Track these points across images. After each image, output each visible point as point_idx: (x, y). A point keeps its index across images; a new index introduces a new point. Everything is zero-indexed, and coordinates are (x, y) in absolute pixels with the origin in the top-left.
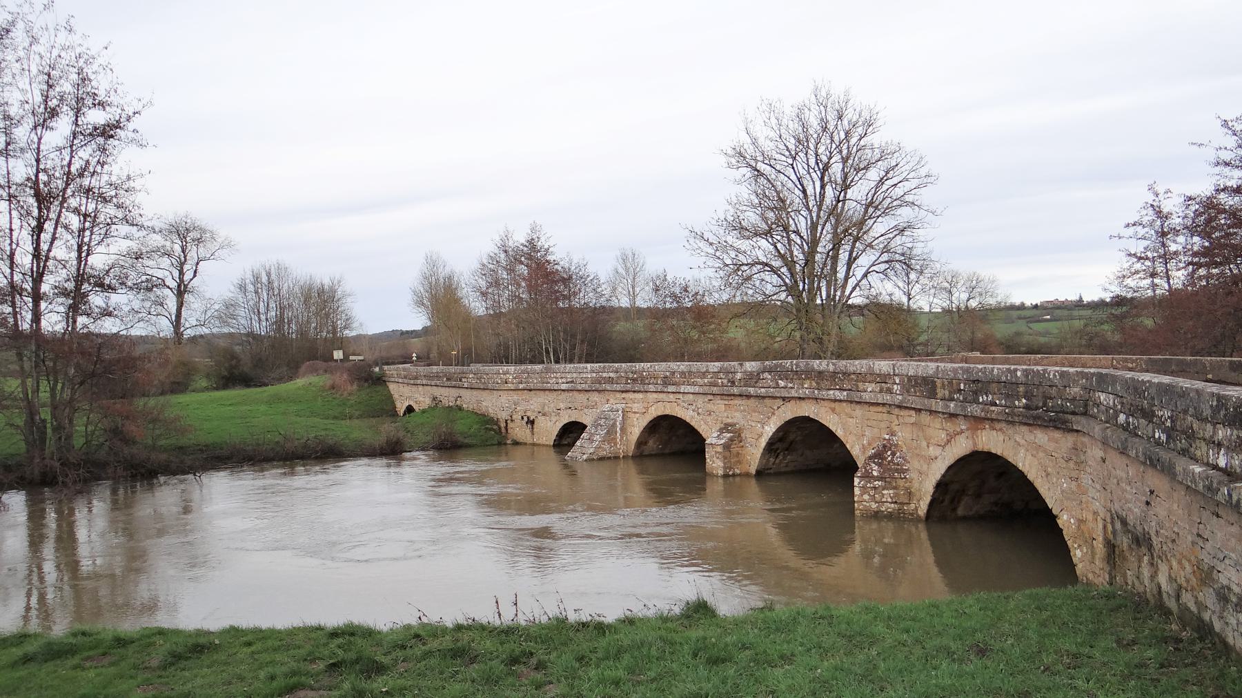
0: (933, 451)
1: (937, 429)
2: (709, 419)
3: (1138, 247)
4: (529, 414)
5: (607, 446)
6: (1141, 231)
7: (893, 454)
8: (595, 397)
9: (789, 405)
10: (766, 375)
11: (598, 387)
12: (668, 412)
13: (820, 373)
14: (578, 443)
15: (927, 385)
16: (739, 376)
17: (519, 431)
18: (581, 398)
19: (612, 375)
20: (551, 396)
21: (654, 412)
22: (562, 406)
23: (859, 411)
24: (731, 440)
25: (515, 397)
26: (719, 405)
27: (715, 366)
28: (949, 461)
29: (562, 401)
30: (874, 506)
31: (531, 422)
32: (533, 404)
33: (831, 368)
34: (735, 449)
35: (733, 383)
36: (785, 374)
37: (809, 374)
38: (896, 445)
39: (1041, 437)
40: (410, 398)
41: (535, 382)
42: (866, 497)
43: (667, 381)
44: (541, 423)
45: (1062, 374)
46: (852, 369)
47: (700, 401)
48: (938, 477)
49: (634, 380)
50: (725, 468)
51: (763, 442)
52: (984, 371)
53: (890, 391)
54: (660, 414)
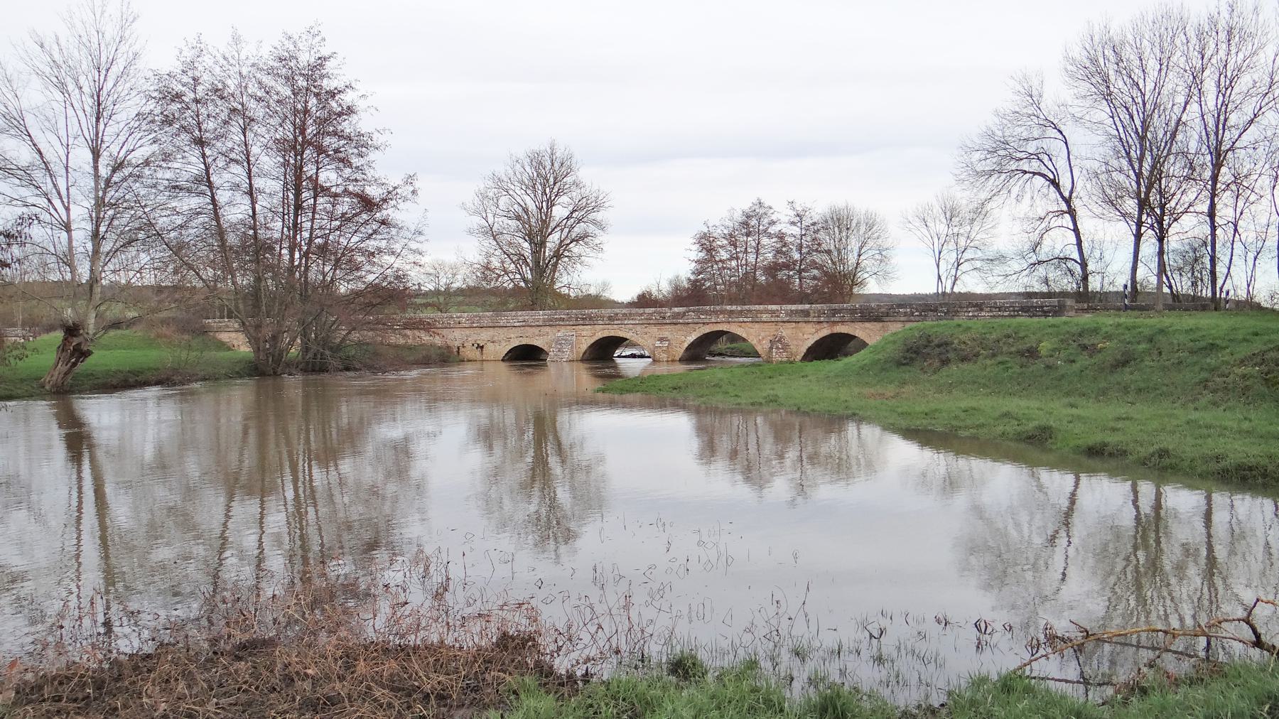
1: (810, 328)
8: (547, 329)
11: (550, 323)
15: (806, 313)
17: (470, 352)
18: (536, 330)
20: (500, 330)
21: (599, 335)
23: (757, 326)
25: (468, 332)
26: (654, 330)
27: (651, 310)
29: (513, 334)
32: (483, 336)
36: (706, 313)
37: (722, 312)
39: (867, 325)
41: (485, 322)
43: (610, 318)
44: (490, 348)
47: (638, 328)
51: (686, 345)
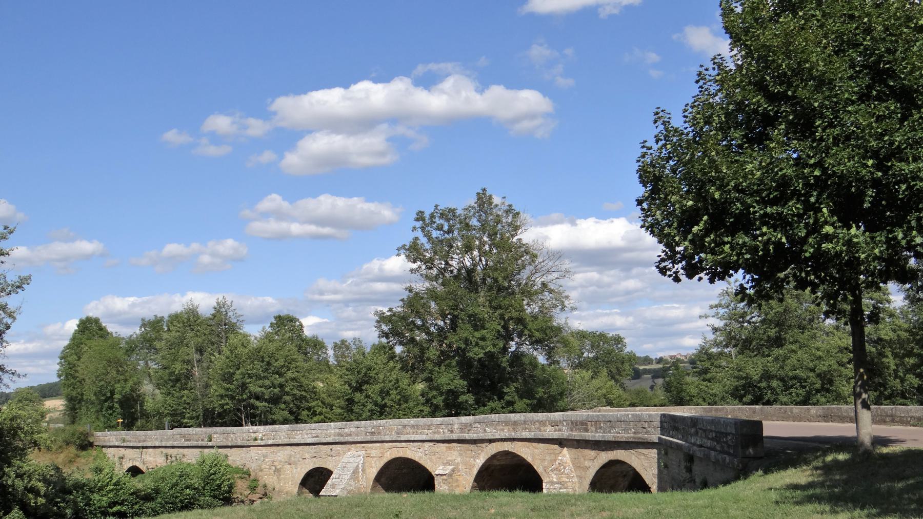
0: (587, 463)
2: (434, 457)
3: (719, 324)
4: (276, 463)
5: (352, 483)
6: (721, 311)
7: (565, 468)
9: (494, 444)
12: (401, 455)
14: (329, 482)
16: (456, 426)
19: (353, 430)
22: (307, 456)
24: (453, 470)
28: (597, 468)
29: (308, 451)
31: (277, 471)
33: (523, 418)
34: (455, 477)
40: (134, 459)
45: (650, 415)
46: (536, 419)
48: (591, 477)
49: (372, 433)
52: (613, 416)
53: (560, 430)
54: (394, 457)
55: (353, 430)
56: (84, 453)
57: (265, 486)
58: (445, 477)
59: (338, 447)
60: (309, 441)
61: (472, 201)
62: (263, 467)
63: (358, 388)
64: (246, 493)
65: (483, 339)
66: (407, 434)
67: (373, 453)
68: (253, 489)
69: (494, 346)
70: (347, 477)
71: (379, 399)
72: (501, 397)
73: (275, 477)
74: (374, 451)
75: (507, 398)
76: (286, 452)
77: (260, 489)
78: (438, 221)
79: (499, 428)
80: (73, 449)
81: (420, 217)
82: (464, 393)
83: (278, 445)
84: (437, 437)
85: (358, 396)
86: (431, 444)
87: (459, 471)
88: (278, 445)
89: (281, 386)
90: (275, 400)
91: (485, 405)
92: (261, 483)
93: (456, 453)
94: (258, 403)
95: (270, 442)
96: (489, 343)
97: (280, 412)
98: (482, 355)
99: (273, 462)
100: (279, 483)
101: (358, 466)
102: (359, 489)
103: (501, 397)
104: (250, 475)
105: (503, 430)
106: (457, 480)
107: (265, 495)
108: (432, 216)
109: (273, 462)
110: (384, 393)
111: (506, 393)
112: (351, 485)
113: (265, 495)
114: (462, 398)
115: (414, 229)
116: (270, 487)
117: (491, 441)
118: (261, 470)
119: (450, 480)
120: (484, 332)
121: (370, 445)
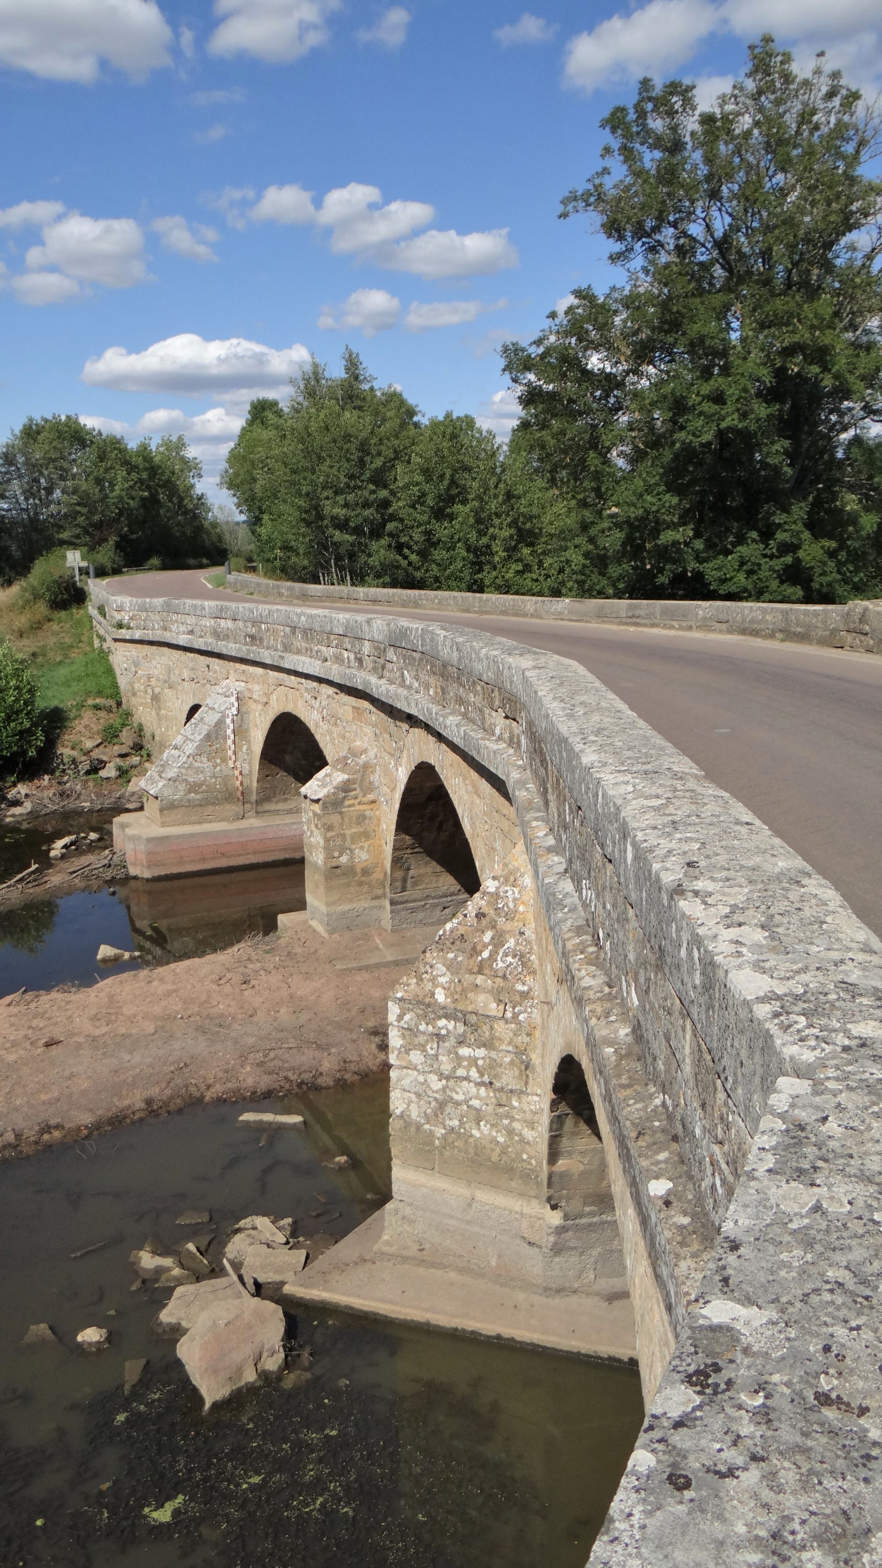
4: (153, 682)
5: (204, 763)
7: (498, 942)
10: (391, 654)
12: (290, 708)
13: (444, 666)
22: (186, 674)
24: (346, 788)
30: (436, 1084)
34: (353, 807)
35: (360, 661)
38: (510, 916)
42: (416, 1057)
50: (328, 850)
55: (230, 624)
56: (63, 614)
57: (140, 729)
58: (317, 808)
59: (215, 663)
60: (183, 640)
61: (751, 79)
62: (136, 686)
63: (439, 514)
64: (89, 744)
65: (718, 398)
66: (298, 652)
67: (257, 690)
68: (111, 735)
69: (744, 415)
70: (190, 748)
71: (473, 536)
72: (767, 535)
73: (154, 713)
74: (256, 687)
75: (781, 536)
76: (164, 660)
77: (127, 737)
78: (657, 124)
79: (423, 676)
80: (42, 608)
81: (615, 121)
82: (672, 526)
83: (151, 643)
84: (335, 672)
85: (442, 530)
86: (331, 690)
87: (370, 788)
88: (151, 643)
89: (385, 504)
90: (377, 533)
91: (727, 552)
92: (136, 720)
93: (368, 730)
94: (338, 536)
95: (138, 635)
96: (729, 407)
97: (379, 552)
98: (707, 437)
99: (149, 678)
100: (160, 726)
101: (220, 724)
102: (226, 779)
103: (767, 535)
104: (119, 704)
105: (427, 687)
106: (362, 818)
107: (138, 747)
108: (642, 115)
109: (149, 678)
110: (481, 522)
111: (779, 525)
112: (198, 771)
113: (138, 747)
114: (667, 537)
115: (607, 150)
116: (147, 732)
117: (412, 720)
118: (134, 694)
119: (335, 819)
120: (718, 381)
121: (251, 669)
